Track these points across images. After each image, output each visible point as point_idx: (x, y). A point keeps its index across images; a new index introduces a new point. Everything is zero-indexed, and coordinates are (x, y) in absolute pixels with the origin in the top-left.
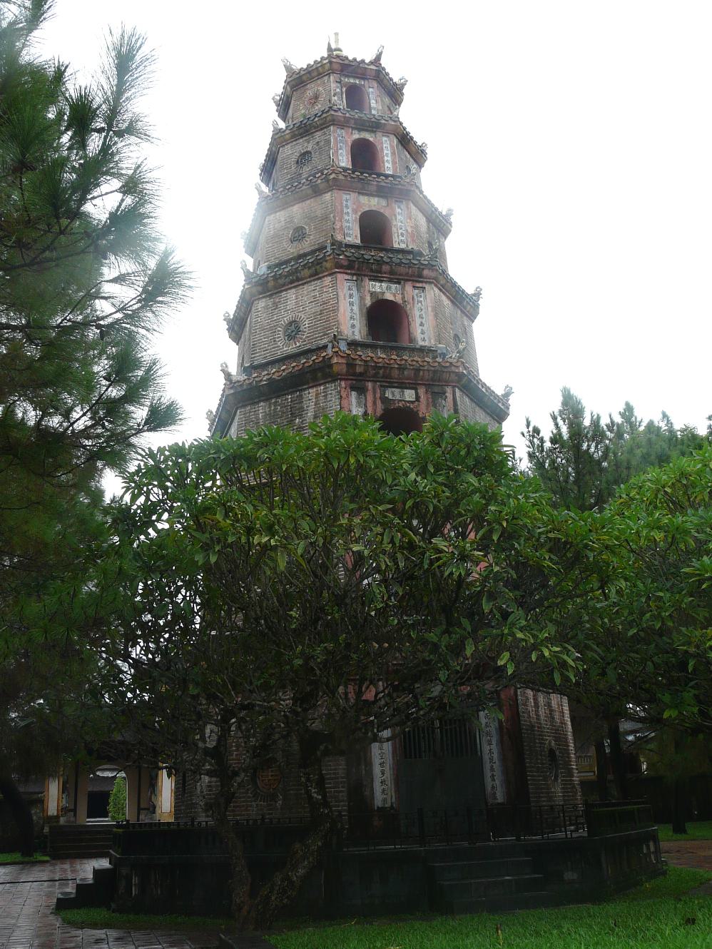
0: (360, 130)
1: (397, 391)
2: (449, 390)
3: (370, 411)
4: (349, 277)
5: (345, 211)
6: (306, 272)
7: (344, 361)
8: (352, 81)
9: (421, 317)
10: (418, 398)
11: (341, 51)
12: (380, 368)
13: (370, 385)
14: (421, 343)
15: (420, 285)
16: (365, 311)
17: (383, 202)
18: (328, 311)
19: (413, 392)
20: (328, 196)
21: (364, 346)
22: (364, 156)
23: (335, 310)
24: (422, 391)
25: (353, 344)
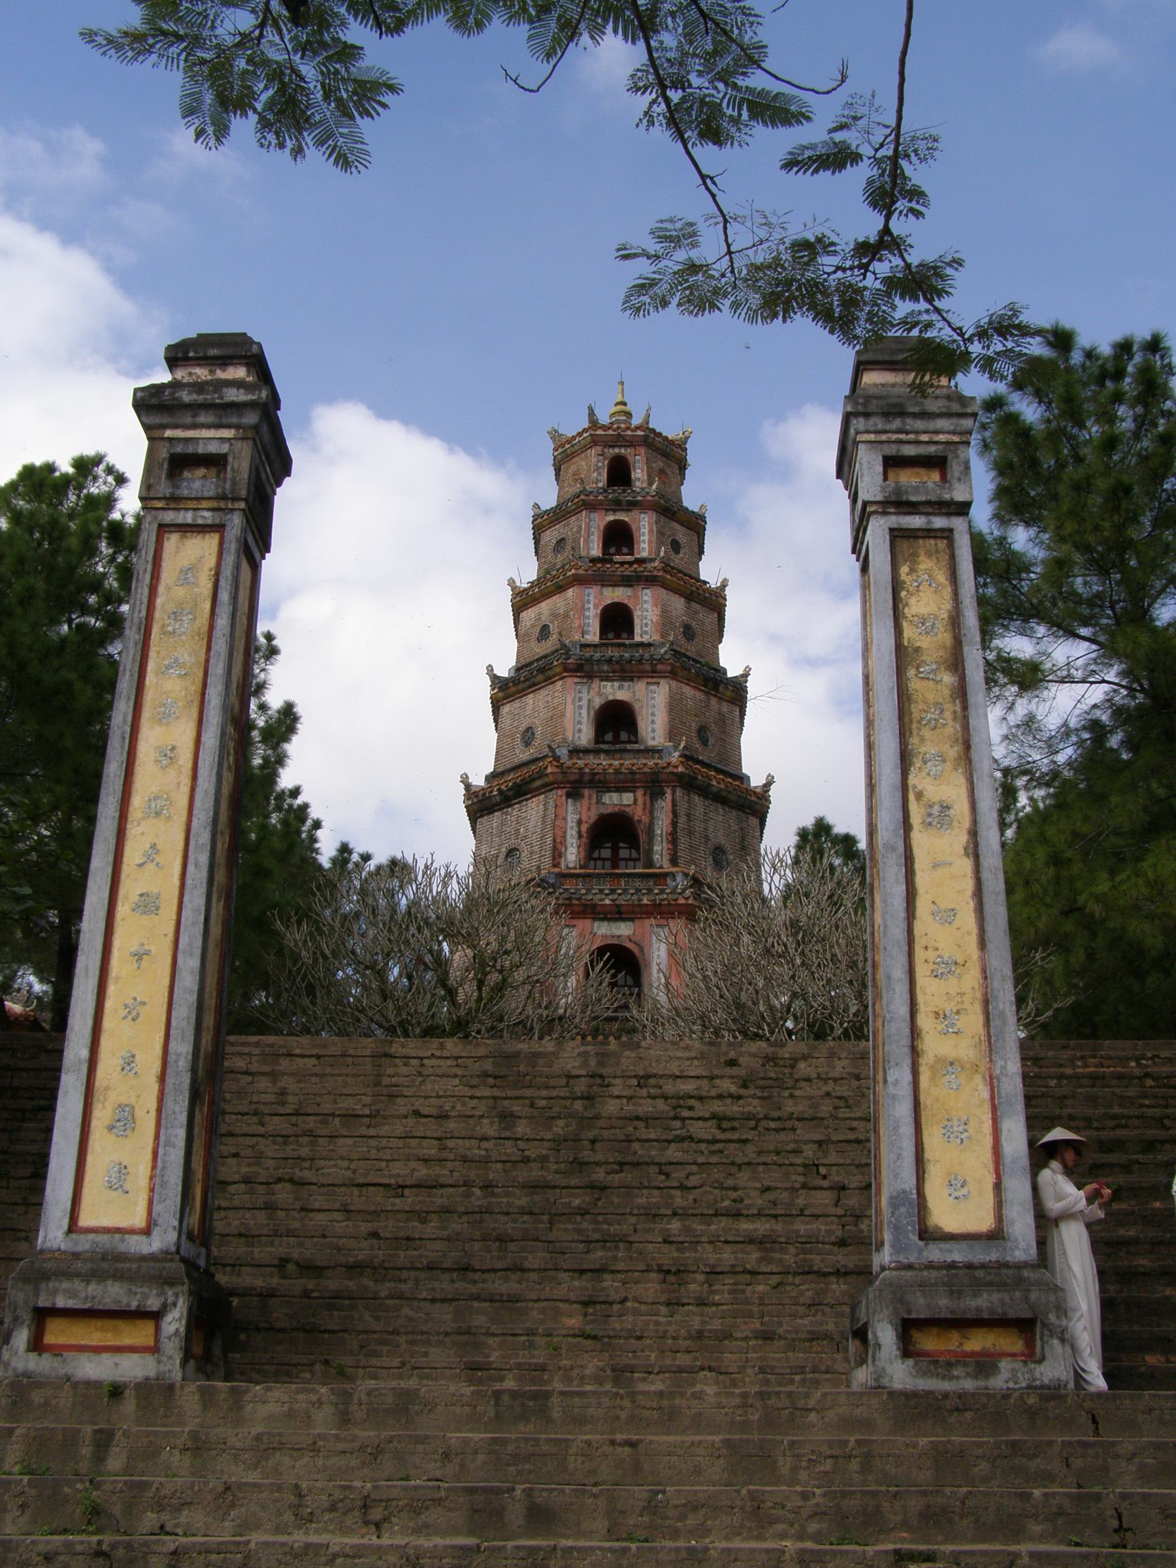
0: (614, 511)
1: (615, 796)
2: (669, 791)
3: (584, 818)
4: (577, 680)
5: (586, 606)
6: (540, 677)
7: (557, 770)
8: (617, 450)
9: (653, 714)
10: (635, 800)
11: (625, 404)
12: (596, 774)
13: (586, 792)
14: (651, 743)
15: (655, 680)
16: (592, 713)
17: (629, 591)
18: (557, 716)
19: (631, 795)
20: (570, 592)
21: (586, 751)
22: (618, 537)
23: (563, 715)
24: (640, 793)
25: (575, 752)
